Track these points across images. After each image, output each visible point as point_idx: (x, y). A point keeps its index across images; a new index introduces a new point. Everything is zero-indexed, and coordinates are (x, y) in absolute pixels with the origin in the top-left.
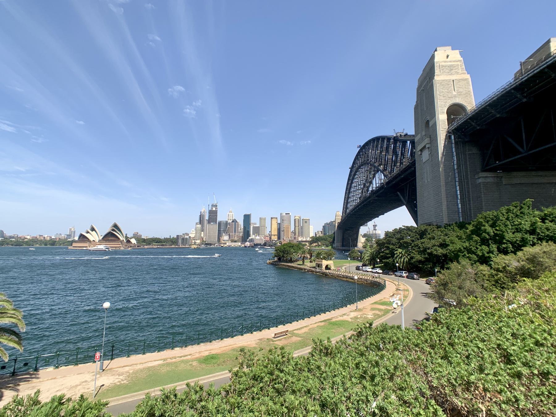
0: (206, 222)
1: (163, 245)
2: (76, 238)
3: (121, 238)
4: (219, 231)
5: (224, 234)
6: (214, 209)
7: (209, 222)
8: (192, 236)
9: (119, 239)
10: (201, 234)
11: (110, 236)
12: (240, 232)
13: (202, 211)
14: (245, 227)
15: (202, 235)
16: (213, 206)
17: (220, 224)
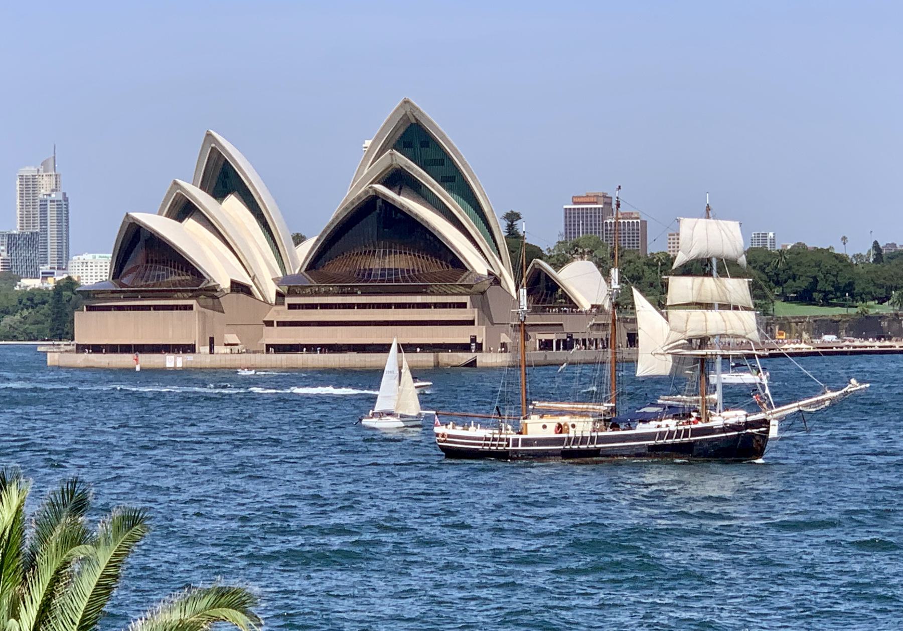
1: (867, 326)
2: (93, 268)
3: (478, 265)
9: (457, 264)
11: (379, 242)
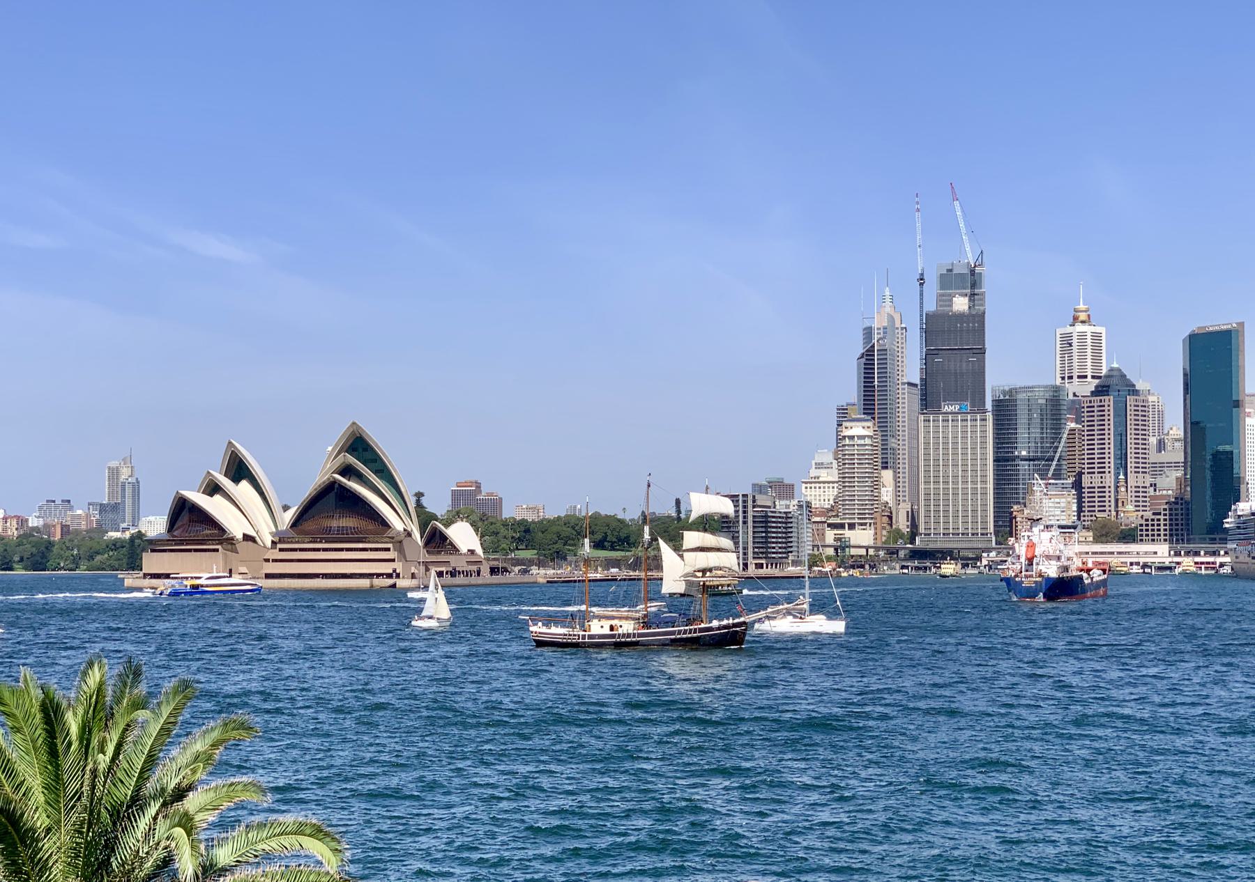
0: (905, 403)
4: (1004, 460)
5: (1039, 485)
6: (961, 304)
7: (928, 398)
8: (821, 497)
10: (876, 485)
12: (1158, 469)
13: (878, 323)
14: (1195, 430)
15: (887, 494)
16: (950, 280)
17: (1005, 411)
